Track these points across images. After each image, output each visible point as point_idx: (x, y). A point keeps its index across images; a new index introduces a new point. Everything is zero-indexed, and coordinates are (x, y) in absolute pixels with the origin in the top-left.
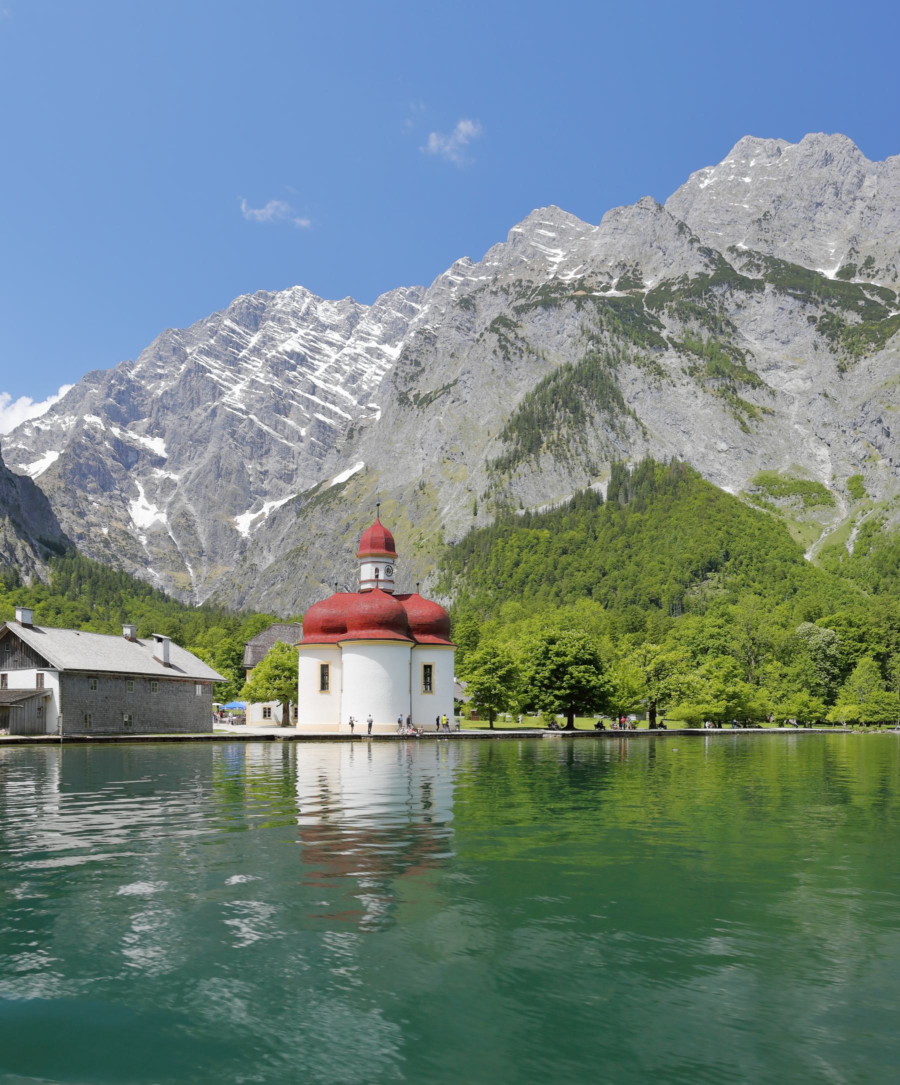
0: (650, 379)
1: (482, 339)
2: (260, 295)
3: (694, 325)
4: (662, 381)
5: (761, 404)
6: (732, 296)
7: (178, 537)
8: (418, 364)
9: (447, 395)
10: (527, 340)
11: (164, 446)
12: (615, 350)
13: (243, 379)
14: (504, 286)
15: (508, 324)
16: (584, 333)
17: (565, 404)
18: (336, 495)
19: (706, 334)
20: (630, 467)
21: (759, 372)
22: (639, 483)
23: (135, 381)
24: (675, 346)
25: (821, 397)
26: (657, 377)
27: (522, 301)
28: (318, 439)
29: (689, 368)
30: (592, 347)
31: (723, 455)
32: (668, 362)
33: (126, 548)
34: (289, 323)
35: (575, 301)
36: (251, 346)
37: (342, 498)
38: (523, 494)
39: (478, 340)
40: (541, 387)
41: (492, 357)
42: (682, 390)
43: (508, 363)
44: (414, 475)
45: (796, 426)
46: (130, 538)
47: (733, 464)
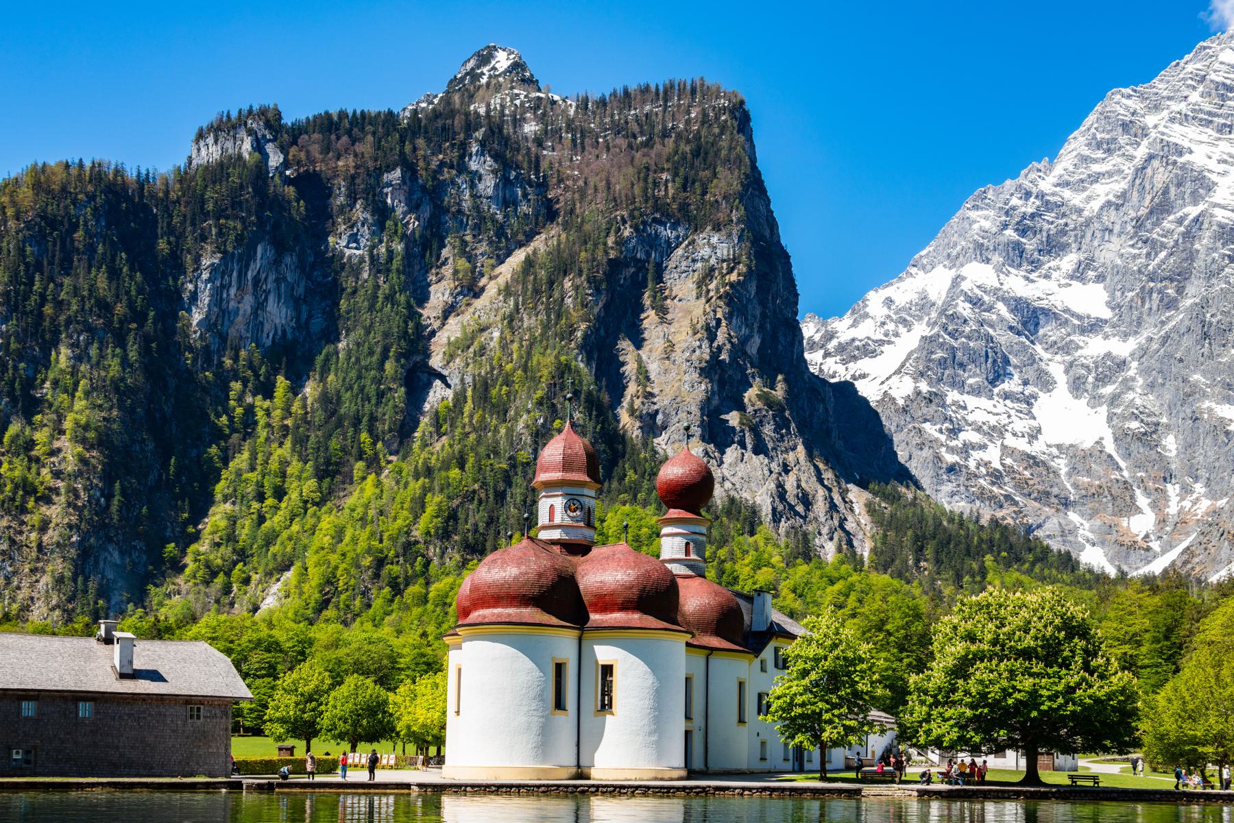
7: (1127, 455)
11: (1105, 296)
23: (1053, 194)
33: (1031, 482)
46: (1037, 464)
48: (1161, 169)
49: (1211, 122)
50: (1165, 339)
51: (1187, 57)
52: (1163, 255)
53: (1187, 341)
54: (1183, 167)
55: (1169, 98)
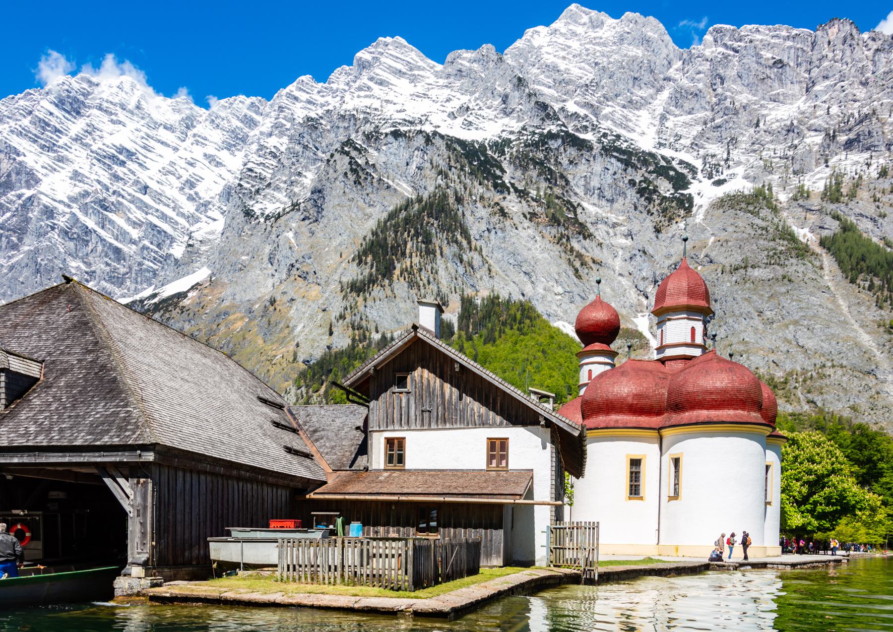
2: (82, 79)
4: (505, 223)
6: (565, 151)
13: (63, 168)
15: (357, 148)
16: (433, 167)
17: (417, 234)
18: (178, 303)
20: (479, 302)
21: (589, 225)
24: (516, 190)
25: (641, 253)
26: (501, 218)
28: (152, 243)
29: (529, 213)
31: (559, 297)
34: (116, 115)
36: (72, 134)
37: (184, 307)
38: (378, 318)
39: (328, 161)
40: (392, 215)
41: (343, 179)
42: (523, 234)
43: (359, 187)
47: (568, 307)
48: (6, 161)
49: (36, 141)
50: (12, 268)
51: (19, 96)
52: (8, 215)
53: (26, 273)
54: (20, 163)
55: (8, 117)
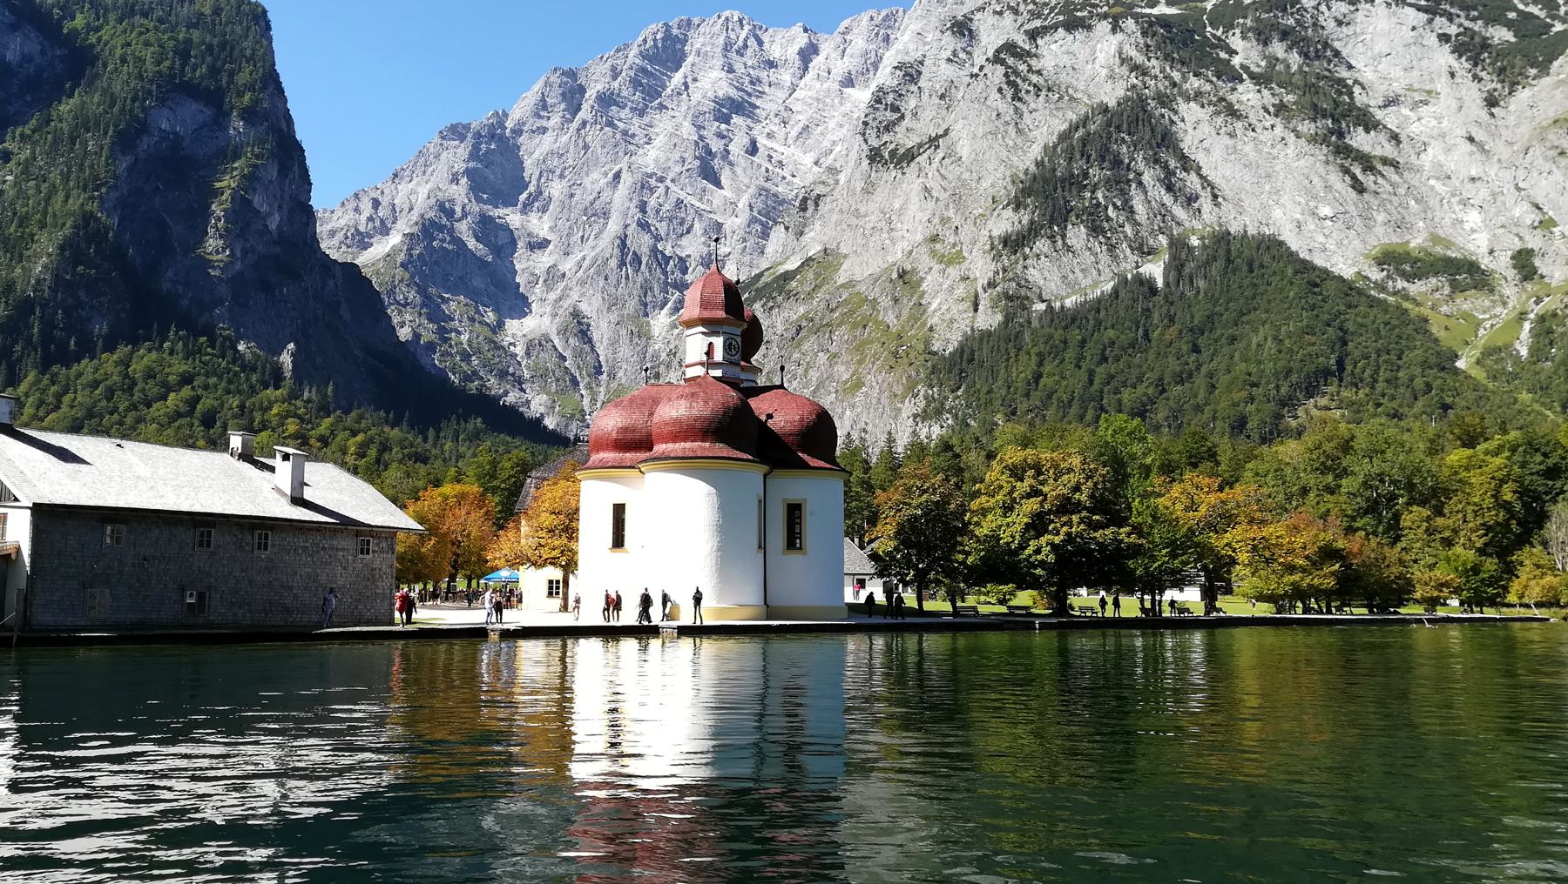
0: (1220, 120)
1: (982, 74)
3: (1278, 48)
5: (1378, 152)
6: (1329, 8)
8: (895, 109)
9: (935, 150)
10: (1045, 72)
12: (1167, 83)
14: (1012, 4)
19: (1295, 59)
20: (1194, 241)
21: (1371, 110)
22: (1208, 263)
24: (1252, 76)
27: (1037, 23)
29: (1274, 105)
30: (1135, 81)
32: (1244, 99)
35: (1110, 20)
38: (1042, 282)
40: (1065, 136)
42: (1265, 136)
44: (891, 260)
45: (1432, 182)
47: (1343, 235)
